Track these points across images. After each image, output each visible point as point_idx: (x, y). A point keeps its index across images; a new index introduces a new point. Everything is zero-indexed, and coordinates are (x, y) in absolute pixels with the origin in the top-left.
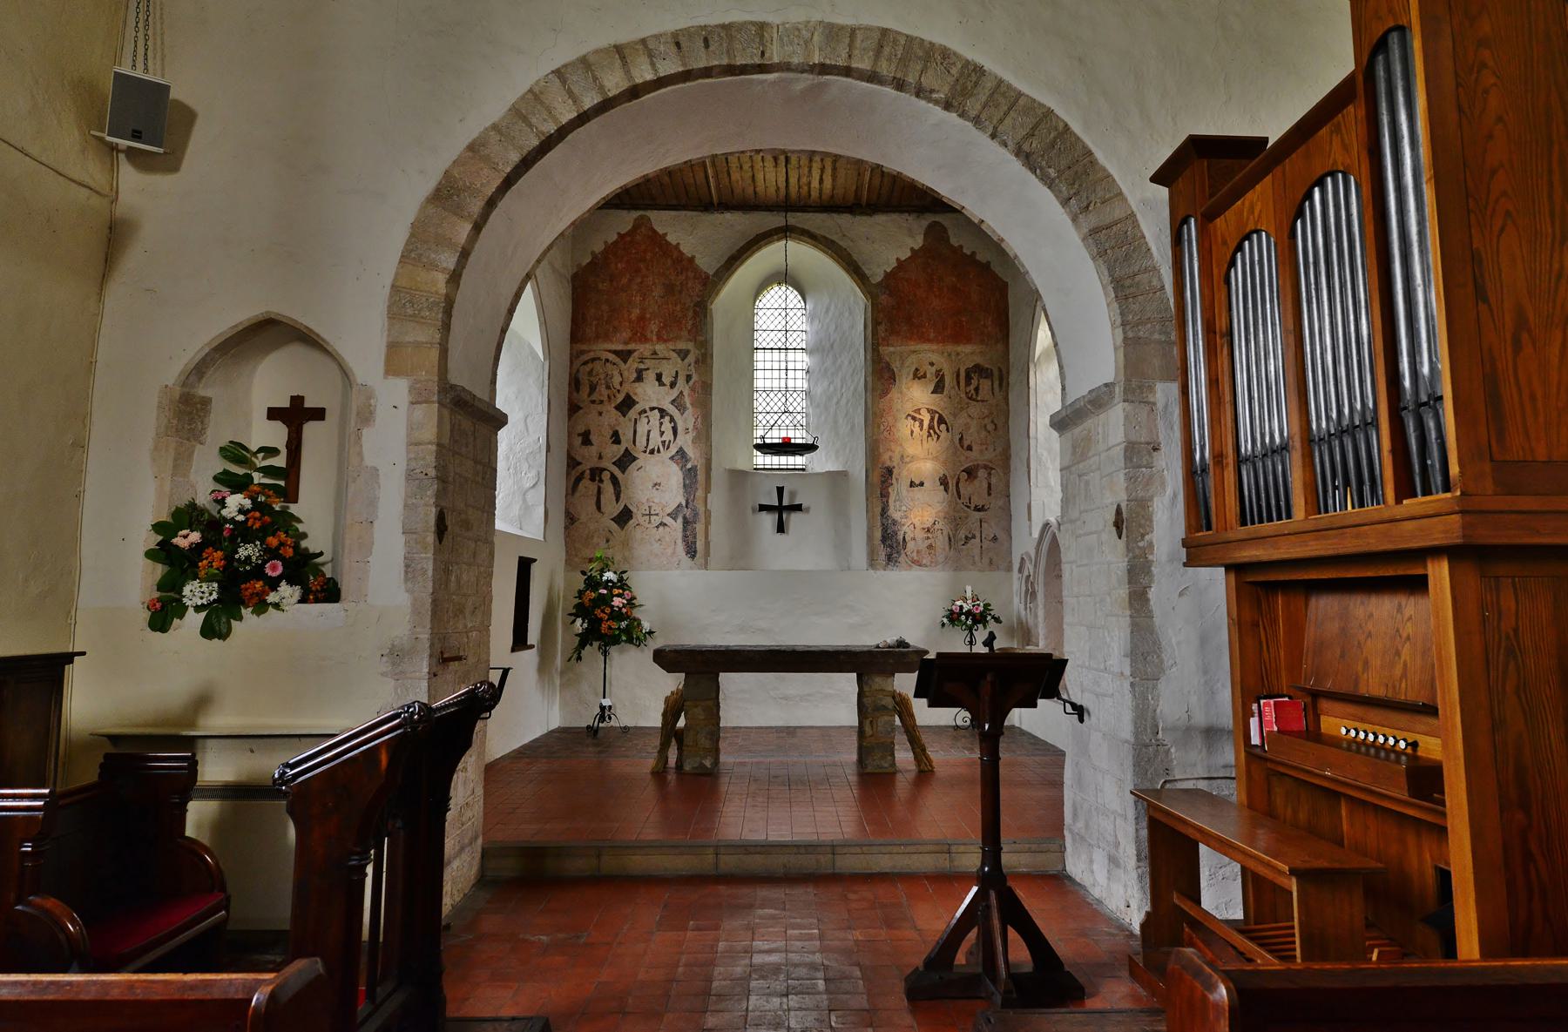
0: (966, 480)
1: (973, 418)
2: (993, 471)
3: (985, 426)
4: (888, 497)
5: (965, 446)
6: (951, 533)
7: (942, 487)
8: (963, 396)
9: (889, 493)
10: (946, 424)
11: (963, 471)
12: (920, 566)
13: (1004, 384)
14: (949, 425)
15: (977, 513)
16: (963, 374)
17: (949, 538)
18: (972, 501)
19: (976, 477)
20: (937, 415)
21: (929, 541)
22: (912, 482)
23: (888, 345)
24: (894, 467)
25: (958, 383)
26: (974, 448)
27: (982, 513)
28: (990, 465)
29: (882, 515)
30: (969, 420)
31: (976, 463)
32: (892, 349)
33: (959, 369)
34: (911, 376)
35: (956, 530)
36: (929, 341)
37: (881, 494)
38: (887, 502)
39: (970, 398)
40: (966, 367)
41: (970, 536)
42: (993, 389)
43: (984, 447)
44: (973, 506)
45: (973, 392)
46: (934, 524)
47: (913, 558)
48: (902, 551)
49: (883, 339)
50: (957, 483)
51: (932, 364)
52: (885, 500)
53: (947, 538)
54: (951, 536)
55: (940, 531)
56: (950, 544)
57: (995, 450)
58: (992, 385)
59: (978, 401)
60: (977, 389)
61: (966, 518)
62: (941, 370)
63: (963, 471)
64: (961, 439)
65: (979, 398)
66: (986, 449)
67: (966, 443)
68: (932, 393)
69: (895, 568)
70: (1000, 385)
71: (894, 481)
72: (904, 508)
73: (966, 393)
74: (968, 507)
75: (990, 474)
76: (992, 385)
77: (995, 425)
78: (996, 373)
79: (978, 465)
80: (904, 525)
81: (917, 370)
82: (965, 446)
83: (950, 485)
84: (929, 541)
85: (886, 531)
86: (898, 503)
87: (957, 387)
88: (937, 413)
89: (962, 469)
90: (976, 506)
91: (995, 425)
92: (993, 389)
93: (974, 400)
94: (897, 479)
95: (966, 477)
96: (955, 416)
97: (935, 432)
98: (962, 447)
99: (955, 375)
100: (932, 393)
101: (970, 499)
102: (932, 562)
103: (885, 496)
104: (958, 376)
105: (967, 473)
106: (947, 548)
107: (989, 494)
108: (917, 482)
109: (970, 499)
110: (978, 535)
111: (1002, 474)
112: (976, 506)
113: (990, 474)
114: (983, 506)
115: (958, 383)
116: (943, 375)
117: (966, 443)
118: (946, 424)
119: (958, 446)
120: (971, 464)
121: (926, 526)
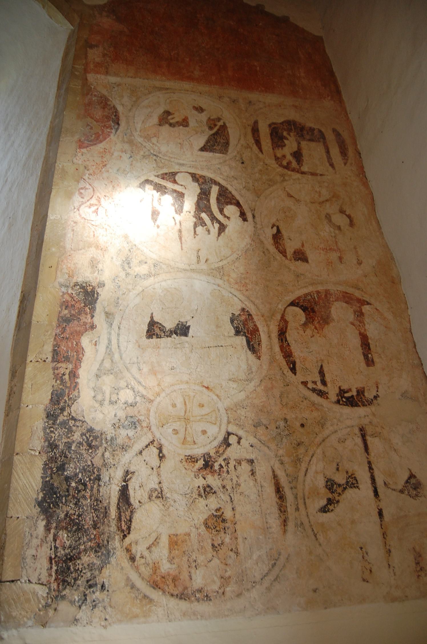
0: (305, 325)
1: (298, 201)
2: (366, 309)
3: (328, 217)
4: (79, 360)
5: (290, 252)
6: (280, 473)
7: (242, 340)
8: (272, 163)
9: (79, 351)
10: (238, 204)
11: (293, 304)
12: (182, 596)
13: (351, 153)
14: (245, 207)
15: (347, 410)
16: (264, 130)
17: (278, 489)
18: (328, 378)
19: (326, 320)
20: (215, 191)
21: (213, 503)
22: (152, 324)
23: (107, 73)
24: (102, 285)
25: (258, 143)
26: (311, 256)
27: (361, 411)
28: (357, 294)
29: (51, 416)
30: (289, 203)
31: (320, 288)
32: (113, 79)
33: (256, 122)
34: (155, 120)
35: (297, 461)
36: (190, 79)
37: (55, 353)
38: (74, 375)
39: (287, 167)
40: (269, 122)
41: (340, 479)
42: (329, 158)
43: (334, 256)
44: (333, 393)
45: (289, 158)
46: (226, 443)
47: (155, 568)
48: (116, 543)
49: (98, 65)
50: (282, 334)
51: (200, 110)
52: (65, 368)
53: (270, 490)
54: (283, 481)
55: (245, 467)
56: (282, 509)
57: (360, 263)
58: (328, 152)
59: (303, 173)
60: (298, 155)
61: (322, 425)
62: (219, 119)
63: (293, 304)
64: (277, 237)
65: (305, 168)
66: (340, 259)
67: (291, 247)
68: (203, 149)
69: (83, 614)
70: (344, 153)
71: (99, 319)
72: (126, 395)
73: (277, 159)
74: (321, 394)
75: (360, 314)
76: (328, 152)
77: (349, 216)
78: (330, 137)
79: (327, 293)
80: (124, 448)
81: (168, 113)
82: (290, 252)
83: (264, 337)
84: (213, 503)
85: (62, 468)
86: (108, 381)
87: (255, 148)
88: (216, 183)
89: (291, 298)
90: (342, 392)
91: (349, 216)
92: (329, 158)
93: (293, 170)
94: (108, 315)
95: (304, 319)
96: (258, 194)
97: (213, 218)
98: (283, 253)
99: (249, 130)
100: (203, 149)
101: (321, 372)
102: (225, 580)
103: (67, 359)
104: (255, 131)
105: (305, 309)
106: (274, 522)
107: (369, 362)
108: (169, 325)
109: (321, 372)
110: (364, 476)
111: (389, 316)
112: (342, 392)
113: (360, 314)
114: (361, 392)
115: (258, 143)
116: (224, 127)
117: (291, 247)
118: (238, 204)
119: (272, 249)
120: (310, 289)
121: (198, 451)
